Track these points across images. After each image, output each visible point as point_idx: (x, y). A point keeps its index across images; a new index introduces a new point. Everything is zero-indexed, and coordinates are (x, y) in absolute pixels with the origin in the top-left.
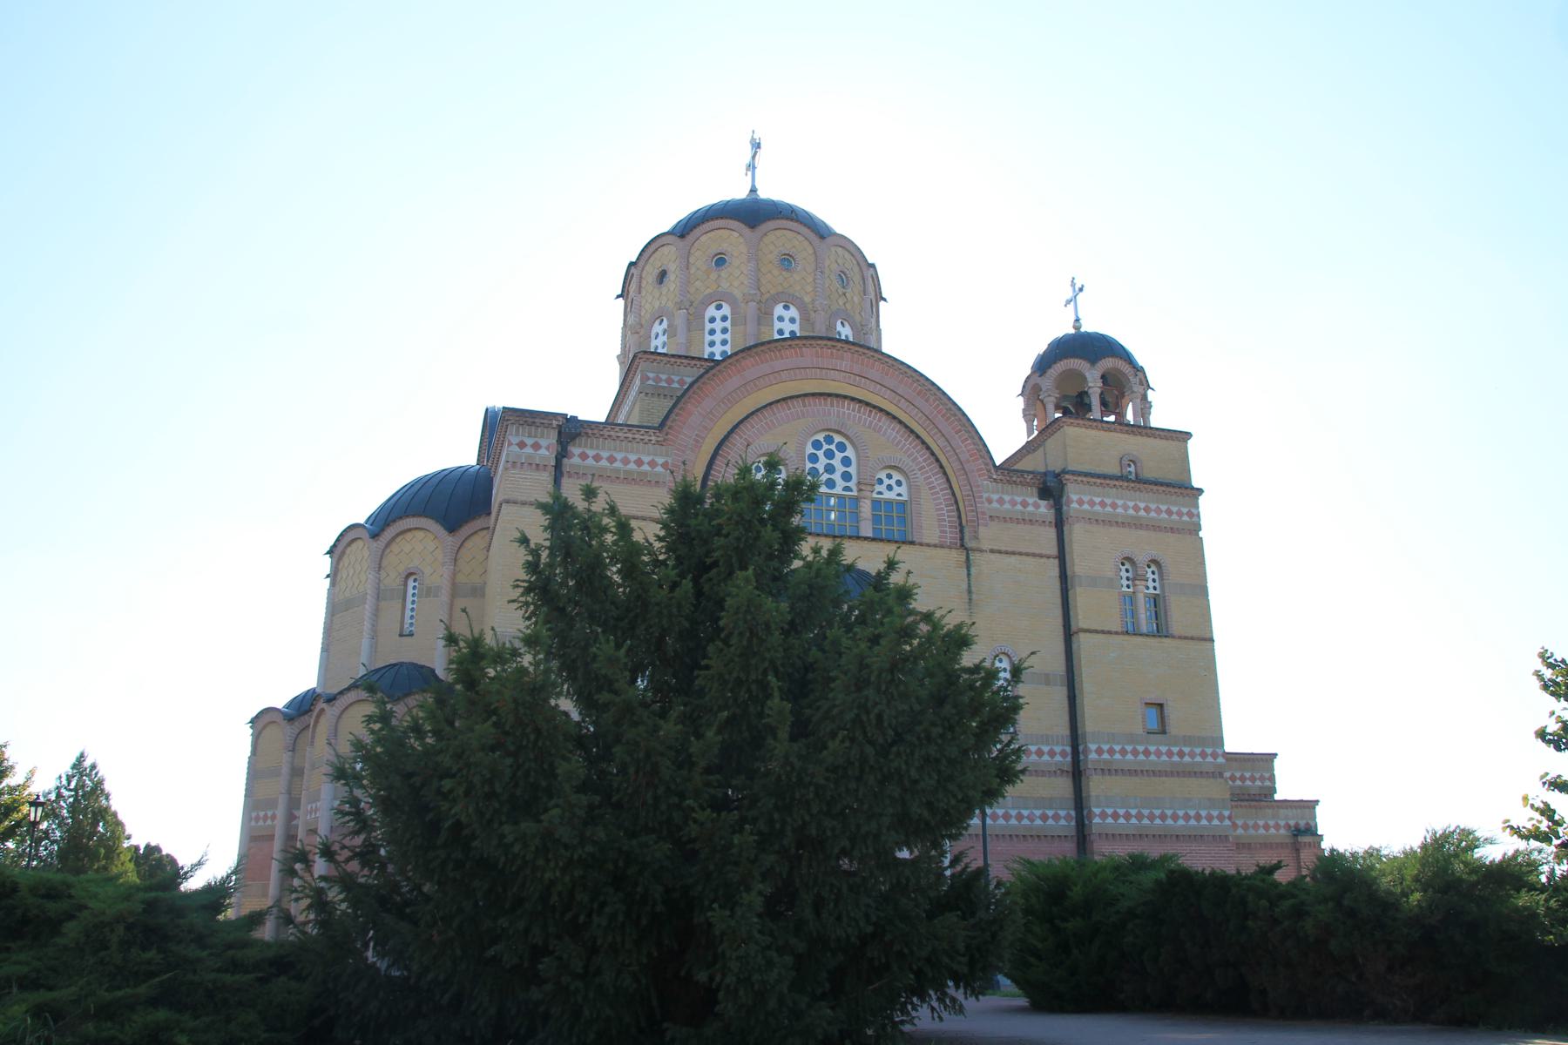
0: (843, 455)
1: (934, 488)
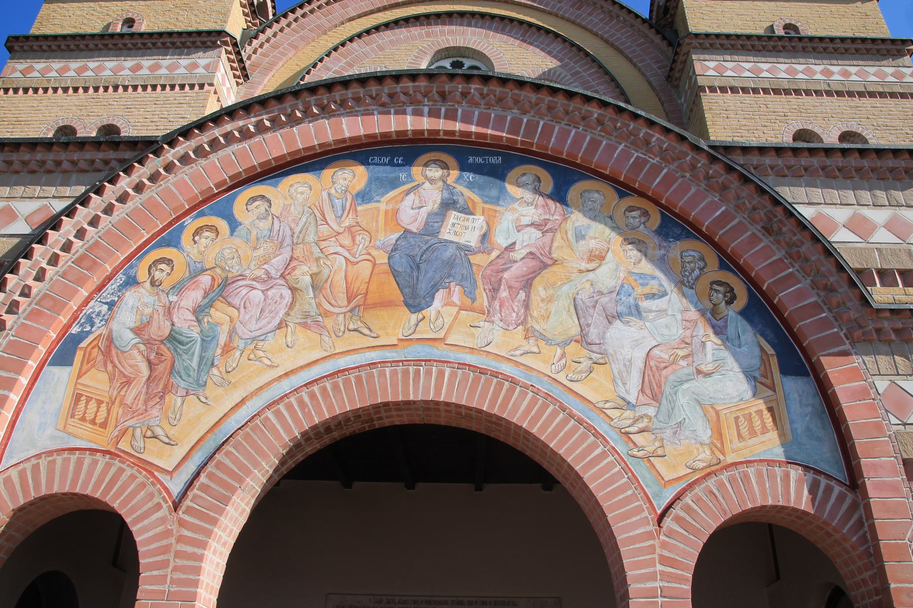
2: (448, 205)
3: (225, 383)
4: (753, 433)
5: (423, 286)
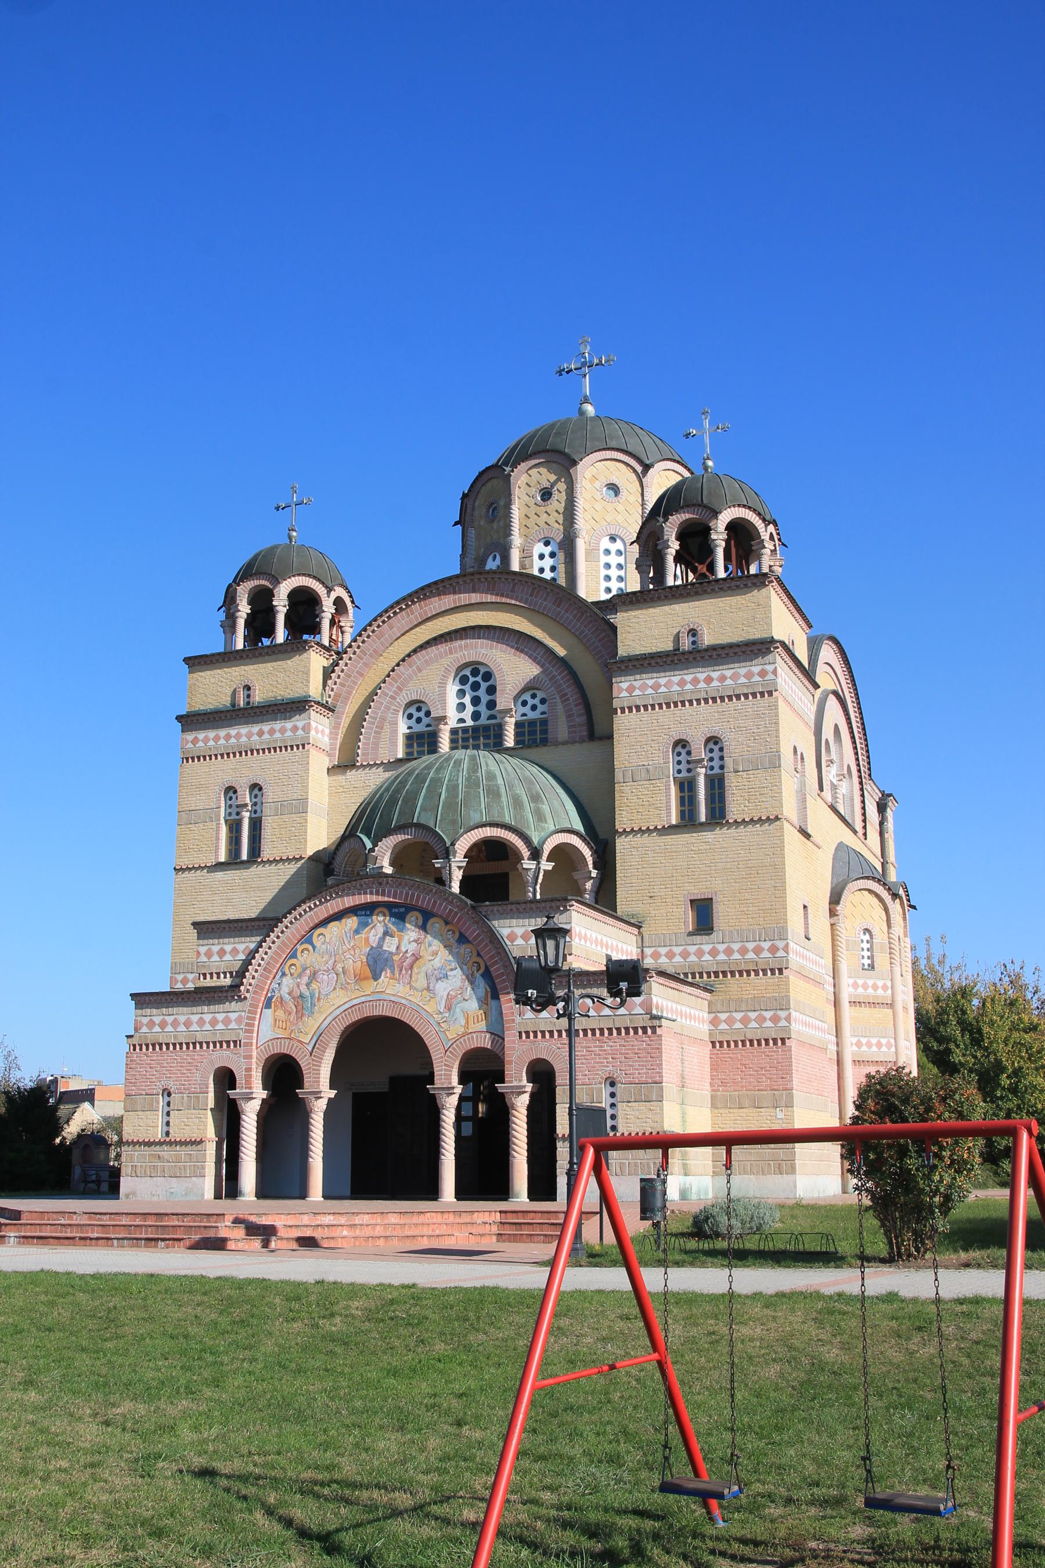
0: (488, 684)
1: (568, 699)
2: (386, 933)
3: (320, 1012)
4: (478, 1022)
5: (378, 970)
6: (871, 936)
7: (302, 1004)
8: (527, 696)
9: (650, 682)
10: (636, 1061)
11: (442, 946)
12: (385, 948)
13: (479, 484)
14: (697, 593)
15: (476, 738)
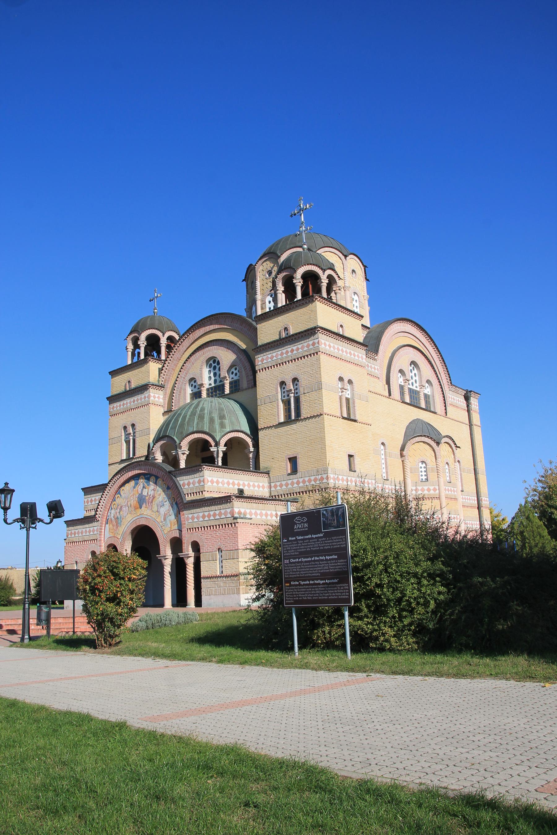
1: (246, 369)
2: (144, 487)
3: (123, 524)
6: (426, 464)
7: (118, 521)
8: (233, 370)
9: (270, 356)
10: (229, 540)
11: (162, 491)
12: (143, 494)
13: (248, 274)
14: (287, 310)
15: (215, 392)
